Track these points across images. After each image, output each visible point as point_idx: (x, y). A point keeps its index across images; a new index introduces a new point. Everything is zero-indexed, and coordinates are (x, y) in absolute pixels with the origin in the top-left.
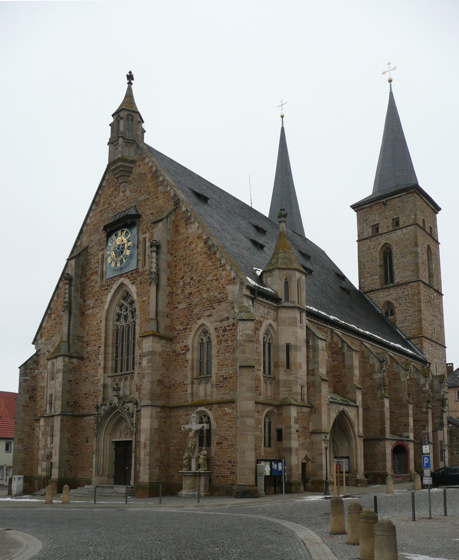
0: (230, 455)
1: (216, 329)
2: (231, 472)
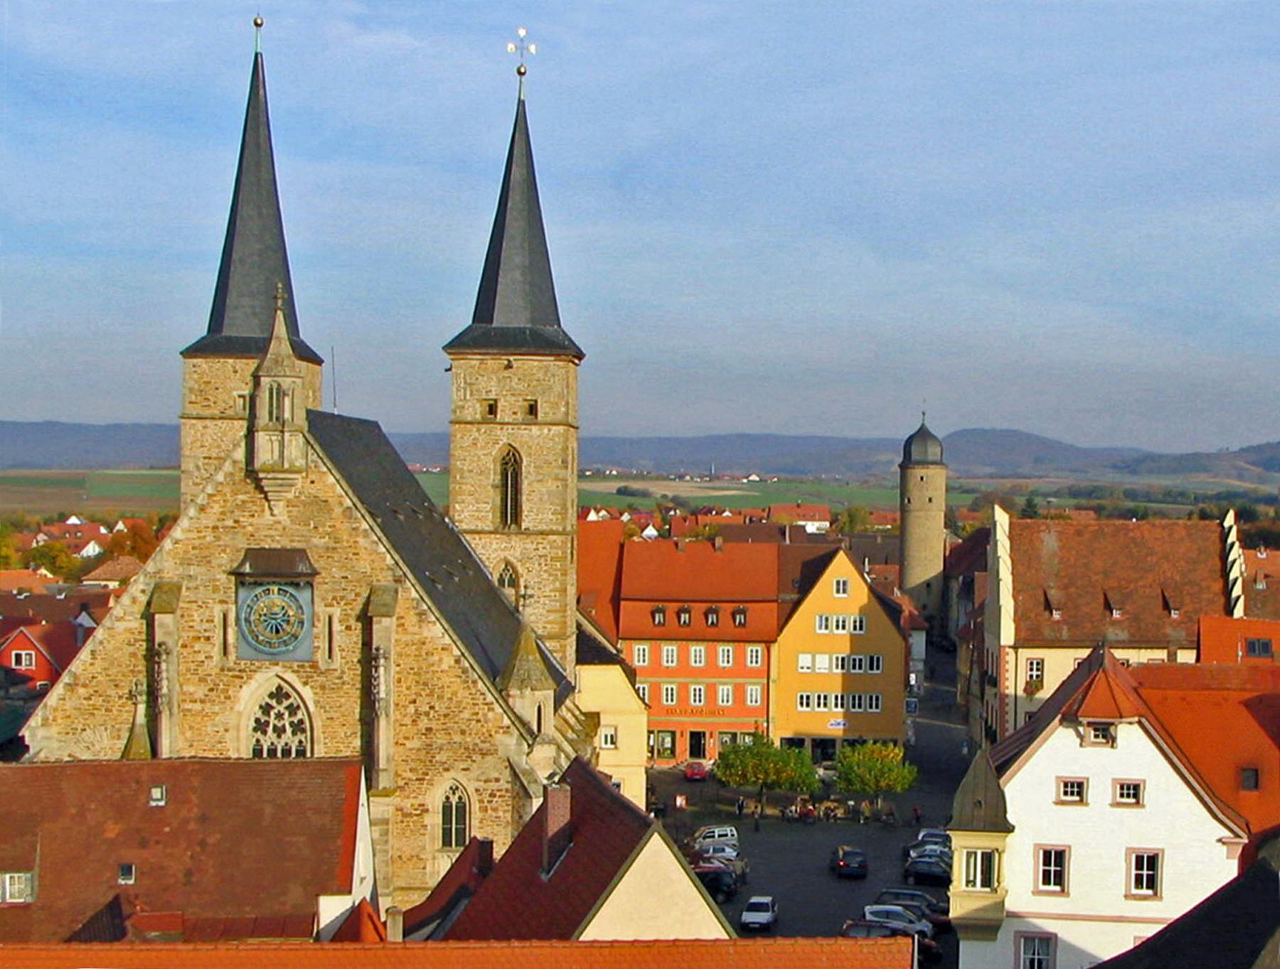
1: (477, 790)
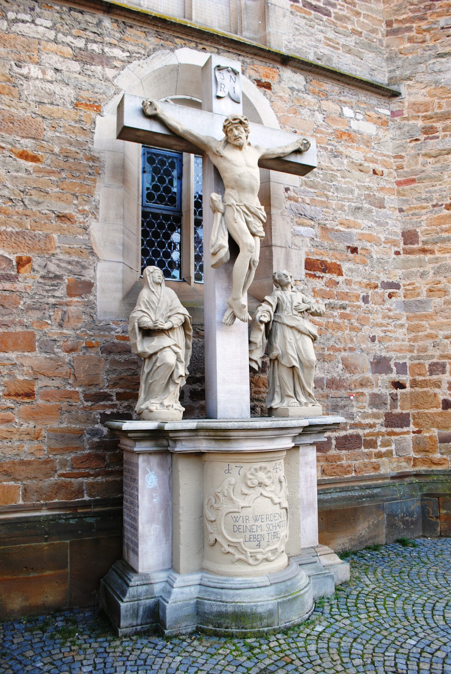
0: (378, 332)
2: (387, 415)
